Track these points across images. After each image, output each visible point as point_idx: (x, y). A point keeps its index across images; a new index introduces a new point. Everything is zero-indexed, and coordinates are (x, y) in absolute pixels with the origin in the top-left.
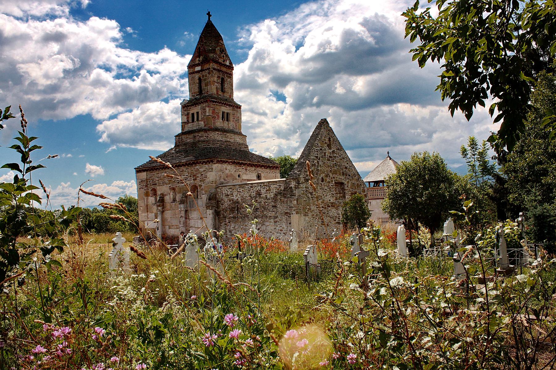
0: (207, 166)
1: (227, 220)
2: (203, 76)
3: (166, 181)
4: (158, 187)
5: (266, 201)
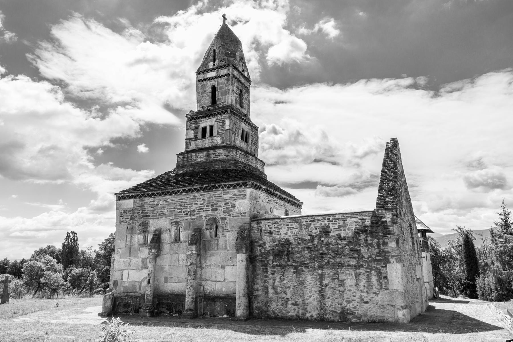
0: (235, 191)
1: (270, 270)
3: (166, 211)
4: (151, 221)
5: (339, 242)
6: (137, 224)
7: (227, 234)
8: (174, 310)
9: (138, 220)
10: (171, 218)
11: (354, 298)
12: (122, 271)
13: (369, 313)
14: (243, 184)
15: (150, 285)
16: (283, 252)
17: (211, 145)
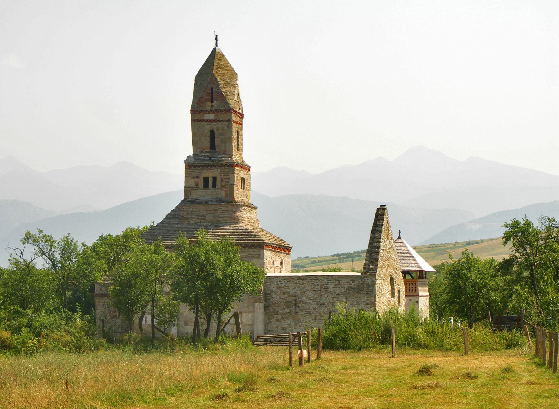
0: (251, 250)
2: (218, 129)
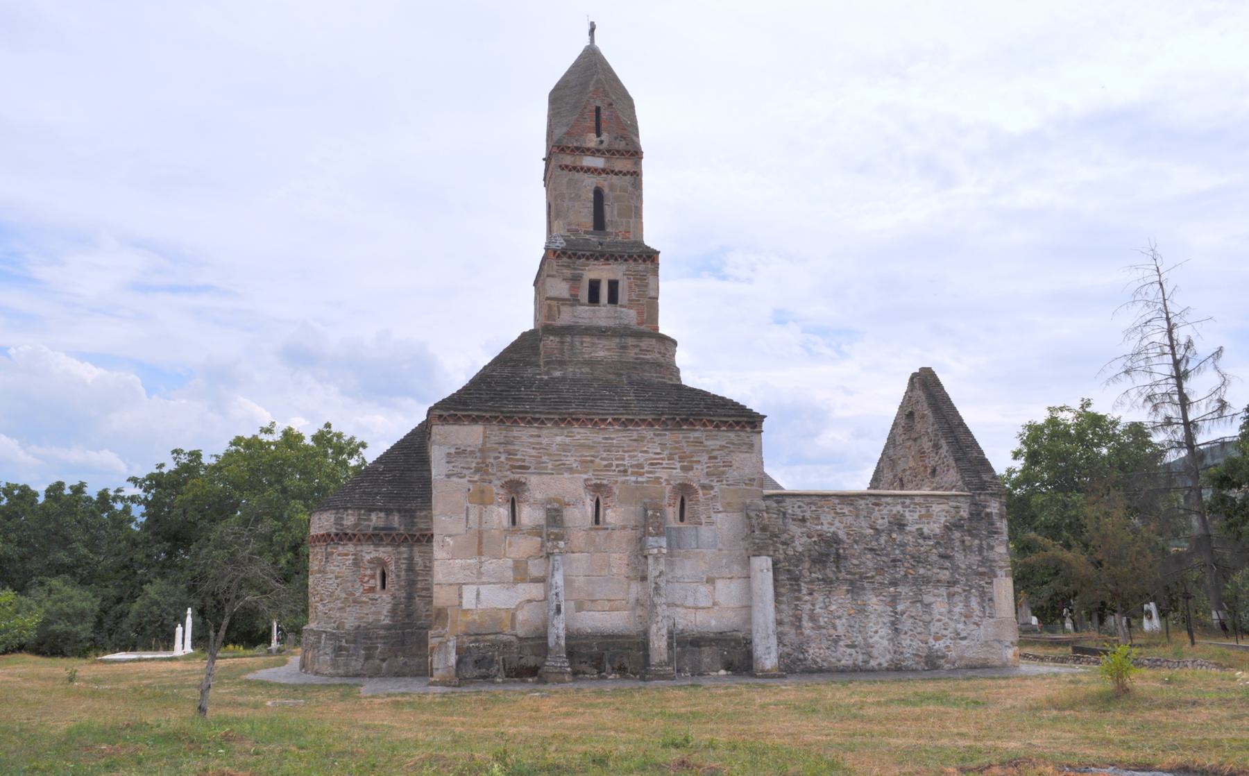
0: (732, 435)
1: (804, 588)
2: (612, 188)
3: (571, 461)
4: (533, 480)
5: (921, 541)
6: (499, 483)
7: (719, 518)
8: (608, 666)
9: (499, 474)
10: (585, 476)
11: (945, 632)
12: (460, 585)
13: (966, 655)
14: (748, 423)
15: (562, 616)
16: (828, 555)
17: (611, 323)
